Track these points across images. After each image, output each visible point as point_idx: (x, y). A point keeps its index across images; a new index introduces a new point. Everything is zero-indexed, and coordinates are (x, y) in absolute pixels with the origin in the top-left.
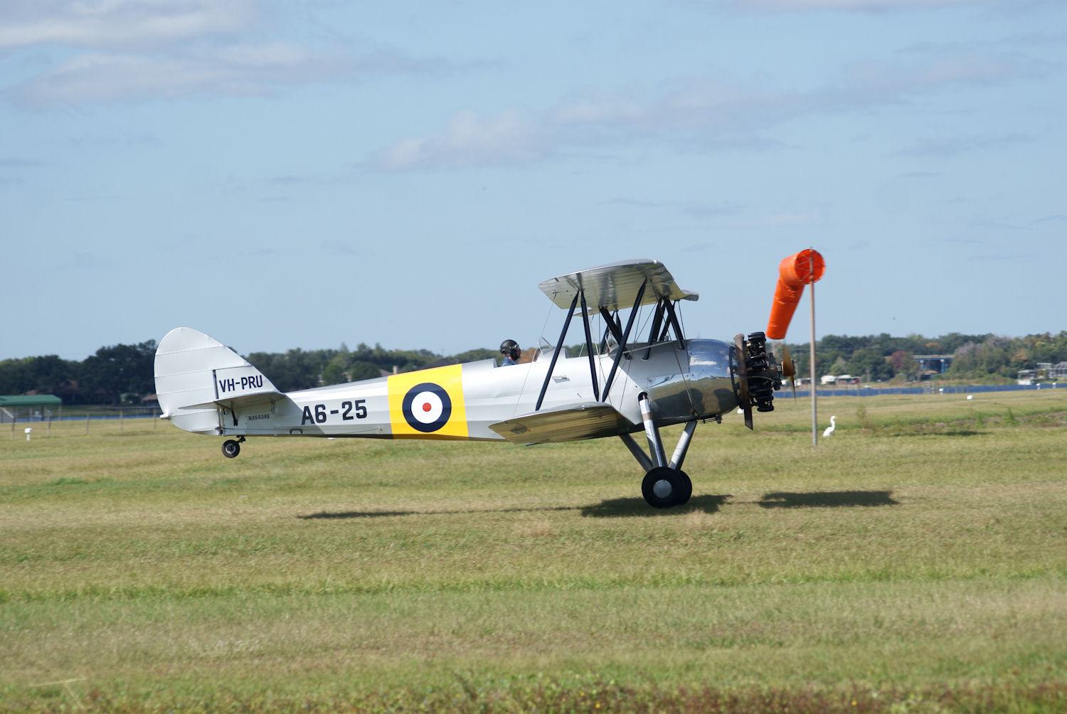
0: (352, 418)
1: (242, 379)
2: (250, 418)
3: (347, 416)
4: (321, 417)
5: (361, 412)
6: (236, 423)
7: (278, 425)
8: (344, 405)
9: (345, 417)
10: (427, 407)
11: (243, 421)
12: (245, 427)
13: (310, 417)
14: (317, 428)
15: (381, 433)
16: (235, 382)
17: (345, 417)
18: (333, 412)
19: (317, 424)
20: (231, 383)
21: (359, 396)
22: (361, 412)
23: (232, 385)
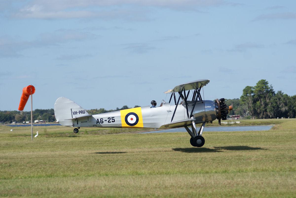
0: (111, 122)
1: (79, 111)
3: (109, 121)
4: (102, 122)
5: (113, 120)
6: (78, 124)
7: (90, 124)
9: (109, 122)
10: (132, 119)
11: (79, 123)
12: (80, 124)
13: (99, 122)
15: (119, 126)
16: (77, 112)
17: (109, 122)
19: (101, 124)
20: (76, 112)
23: (76, 113)
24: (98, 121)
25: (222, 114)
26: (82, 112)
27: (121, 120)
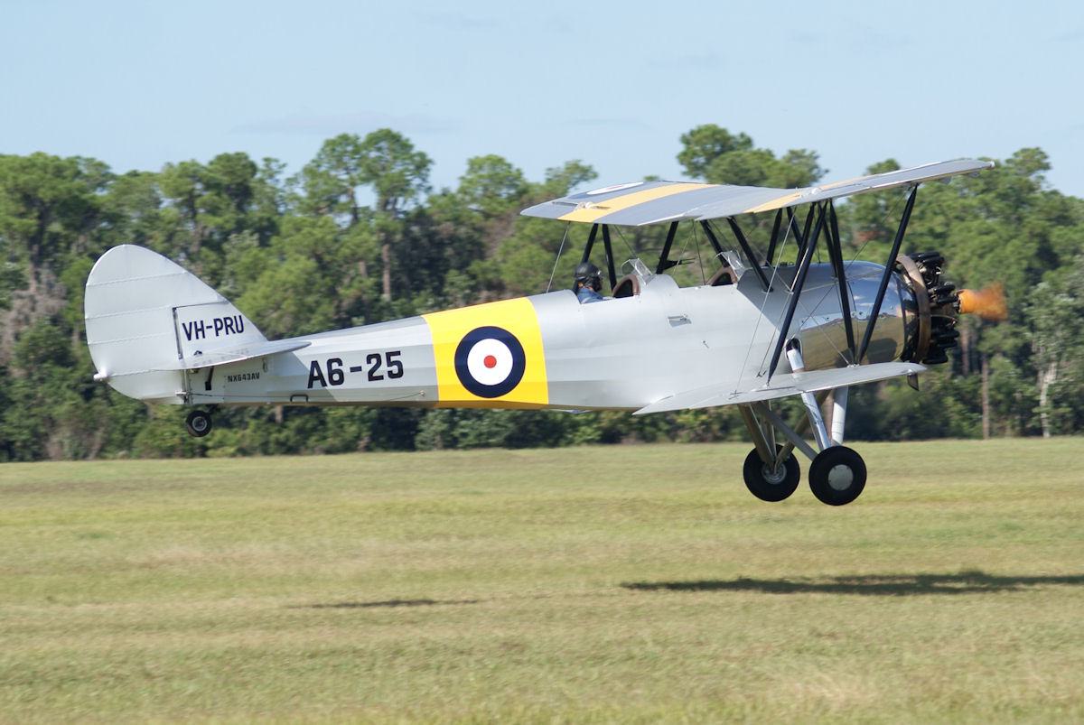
0: (381, 378)
1: (216, 320)
2: (230, 379)
3: (375, 375)
4: (336, 377)
5: (395, 369)
6: (208, 387)
9: (371, 377)
10: (490, 362)
12: (222, 392)
13: (321, 377)
14: (328, 394)
16: (205, 326)
17: (371, 377)
18: (353, 370)
19: (329, 387)
20: (199, 327)
21: (392, 347)
23: (201, 330)
24: (316, 374)
25: (934, 331)
26: (230, 326)
27: (434, 369)
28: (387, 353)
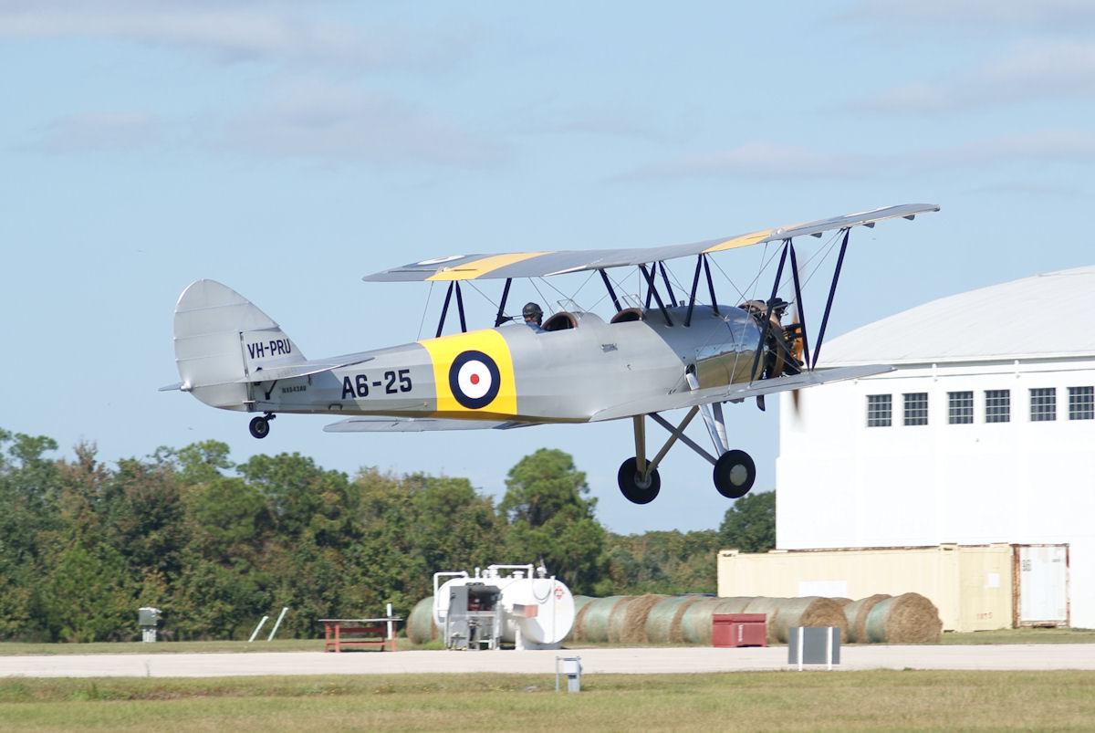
0: (395, 391)
1: (271, 342)
3: (391, 388)
4: (363, 390)
5: (405, 384)
6: (268, 396)
8: (387, 375)
9: (389, 391)
10: (475, 379)
14: (355, 404)
17: (389, 391)
19: (358, 398)
20: (260, 348)
21: (403, 366)
22: (405, 384)
24: (348, 387)
27: (434, 384)
28: (400, 372)
